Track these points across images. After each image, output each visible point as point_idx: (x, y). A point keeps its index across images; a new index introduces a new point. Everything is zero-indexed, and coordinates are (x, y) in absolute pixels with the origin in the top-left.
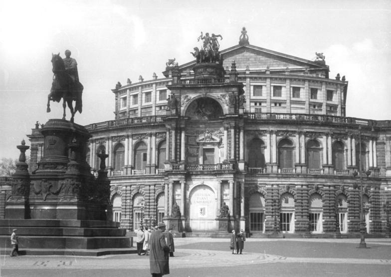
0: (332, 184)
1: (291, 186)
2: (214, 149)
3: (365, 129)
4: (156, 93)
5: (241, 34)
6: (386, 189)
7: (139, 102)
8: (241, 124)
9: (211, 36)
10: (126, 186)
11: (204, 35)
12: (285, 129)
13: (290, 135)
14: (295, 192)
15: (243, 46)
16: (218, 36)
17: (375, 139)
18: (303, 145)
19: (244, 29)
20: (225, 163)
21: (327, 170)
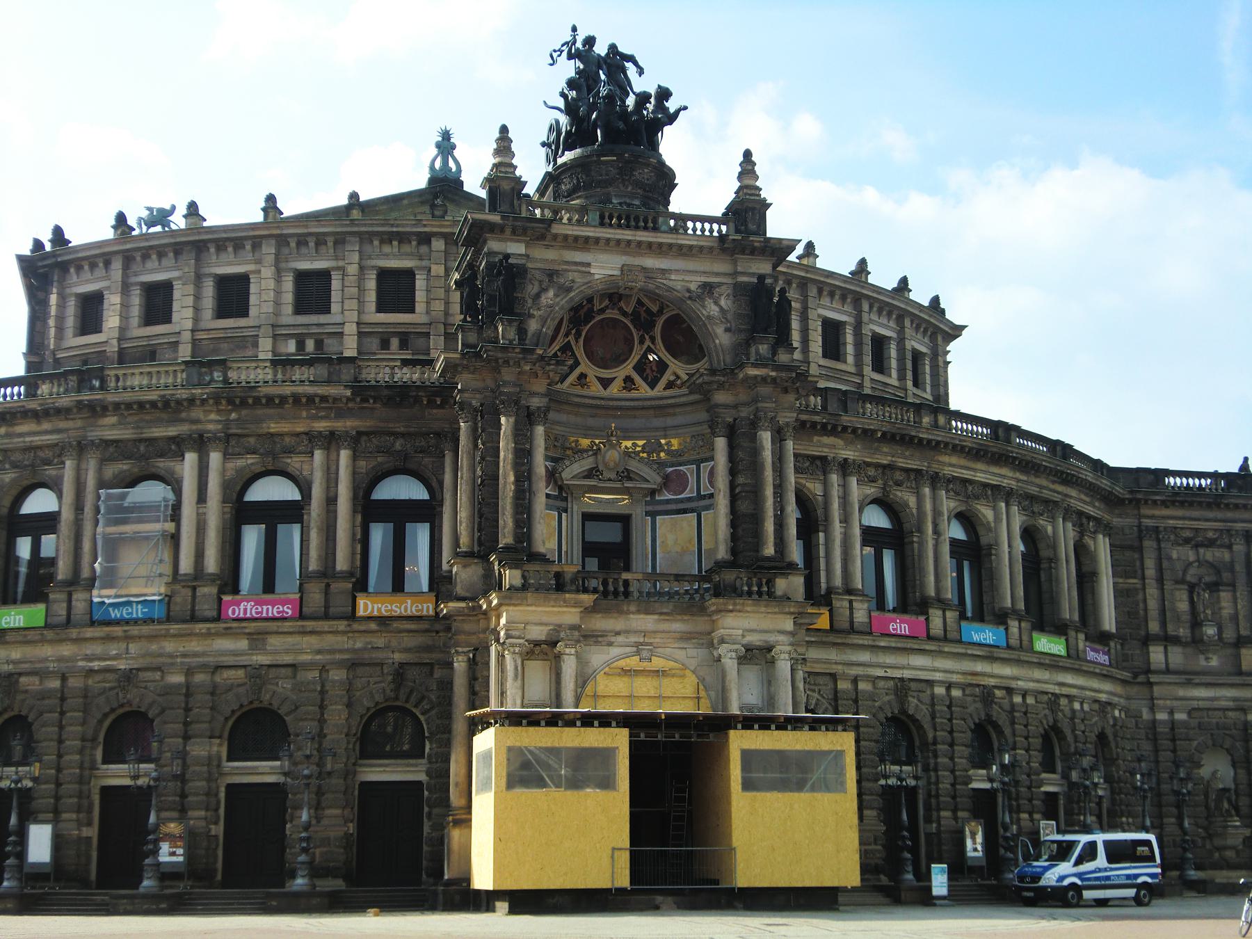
0: (1031, 685)
1: (913, 685)
2: (624, 520)
4: (278, 279)
5: (435, 151)
6: (1146, 715)
9: (601, 49)
10: (189, 672)
11: (579, 45)
12: (885, 461)
13: (898, 484)
17: (1108, 530)
19: (446, 135)
21: (1014, 625)
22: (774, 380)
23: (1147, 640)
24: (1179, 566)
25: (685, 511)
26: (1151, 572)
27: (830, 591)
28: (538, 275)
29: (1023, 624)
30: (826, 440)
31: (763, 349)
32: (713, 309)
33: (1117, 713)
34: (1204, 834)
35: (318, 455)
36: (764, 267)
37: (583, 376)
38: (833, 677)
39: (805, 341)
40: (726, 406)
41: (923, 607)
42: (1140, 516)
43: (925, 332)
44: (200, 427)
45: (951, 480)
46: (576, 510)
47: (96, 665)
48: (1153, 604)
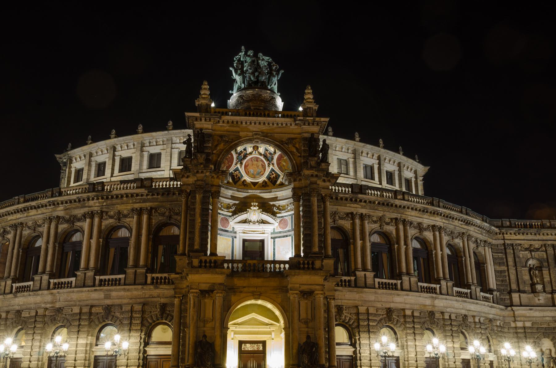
0: (453, 310)
7: (108, 172)
22: (317, 176)
23: (510, 292)
24: (524, 261)
25: (287, 236)
26: (511, 263)
29: (449, 284)
30: (352, 205)
31: (313, 163)
33: (498, 324)
35: (135, 217)
38: (357, 307)
41: (399, 276)
42: (504, 239)
43: (411, 170)
44: (92, 208)
45: (411, 223)
48: (513, 277)
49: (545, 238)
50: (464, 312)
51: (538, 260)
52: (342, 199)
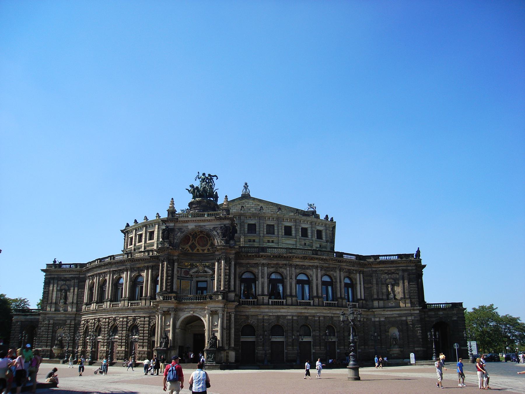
0: (322, 315)
2: (206, 281)
3: (350, 262)
4: (158, 231)
6: (373, 320)
7: (143, 240)
8: (232, 256)
9: (207, 176)
11: (201, 175)
12: (275, 262)
13: (281, 268)
14: (285, 322)
15: (246, 196)
16: (214, 176)
18: (294, 277)
20: (217, 294)
21: (316, 300)
22: (224, 249)
26: (375, 282)
27: (259, 295)
28: (177, 230)
32: (215, 233)
34: (388, 350)
36: (227, 222)
37: (198, 249)
39: (278, 232)
40: (217, 255)
46: (195, 279)
47: (110, 316)
49: (398, 265)
50: (330, 315)
51: (393, 279)
52: (250, 256)
